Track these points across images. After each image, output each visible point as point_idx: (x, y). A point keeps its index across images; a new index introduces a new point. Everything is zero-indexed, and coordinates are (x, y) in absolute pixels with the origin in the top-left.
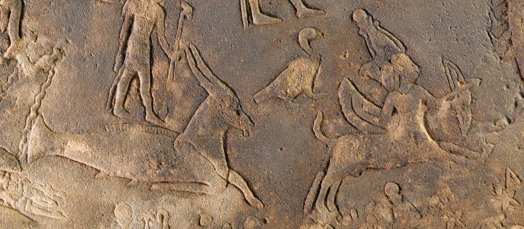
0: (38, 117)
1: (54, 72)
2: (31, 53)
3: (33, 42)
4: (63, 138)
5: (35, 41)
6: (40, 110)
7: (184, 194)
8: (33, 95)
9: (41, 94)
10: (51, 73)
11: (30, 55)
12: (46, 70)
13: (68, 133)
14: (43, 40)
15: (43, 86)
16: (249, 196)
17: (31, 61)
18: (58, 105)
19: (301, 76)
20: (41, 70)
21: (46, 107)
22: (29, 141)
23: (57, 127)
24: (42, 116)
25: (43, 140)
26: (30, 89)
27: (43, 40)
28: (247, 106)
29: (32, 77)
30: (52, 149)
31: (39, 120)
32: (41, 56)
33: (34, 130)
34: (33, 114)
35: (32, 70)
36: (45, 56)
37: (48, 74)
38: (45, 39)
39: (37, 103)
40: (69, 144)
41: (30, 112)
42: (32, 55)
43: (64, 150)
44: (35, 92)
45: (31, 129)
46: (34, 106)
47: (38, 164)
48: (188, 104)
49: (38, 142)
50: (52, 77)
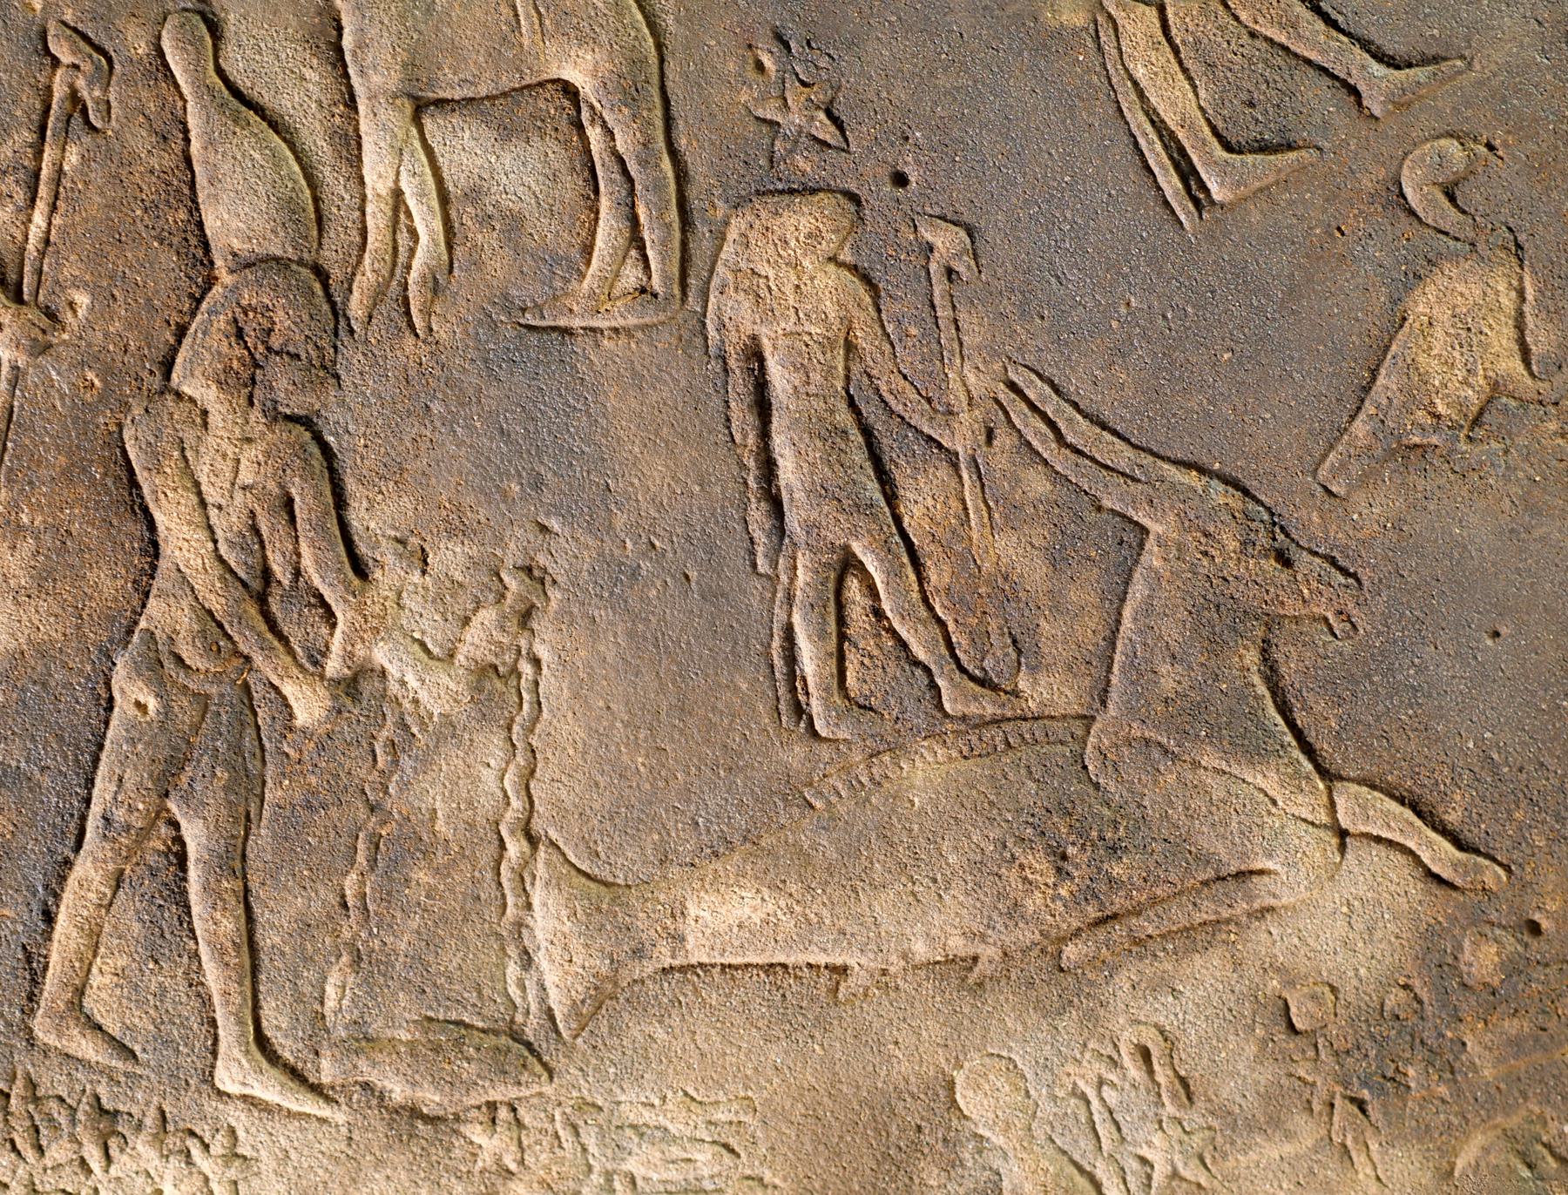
0: (542, 853)
1: (536, 662)
2: (425, 624)
3: (416, 577)
4: (662, 897)
5: (424, 572)
6: (537, 826)
7: (1193, 938)
8: (489, 777)
9: (520, 759)
10: (526, 668)
11: (423, 633)
12: (504, 664)
13: (674, 871)
14: (450, 557)
15: (516, 728)
16: (1439, 853)
17: (436, 650)
18: (599, 778)
19: (1467, 332)
20: (485, 671)
21: (557, 804)
22: (541, 959)
23: (626, 863)
24: (553, 844)
25: (591, 930)
26: (471, 760)
27: (450, 557)
28: (1308, 520)
29: (462, 713)
30: (638, 953)
31: (548, 863)
32: (466, 621)
33: (545, 904)
34: (515, 848)
35: (452, 685)
36: (482, 613)
37: (519, 676)
38: (458, 550)
39: (516, 803)
40: (692, 910)
41: (502, 845)
42: (432, 629)
43: (683, 939)
44: (492, 763)
45: (529, 906)
46: (509, 815)
47: (605, 1030)
48: (1083, 593)
49: (576, 944)
50: (537, 684)
